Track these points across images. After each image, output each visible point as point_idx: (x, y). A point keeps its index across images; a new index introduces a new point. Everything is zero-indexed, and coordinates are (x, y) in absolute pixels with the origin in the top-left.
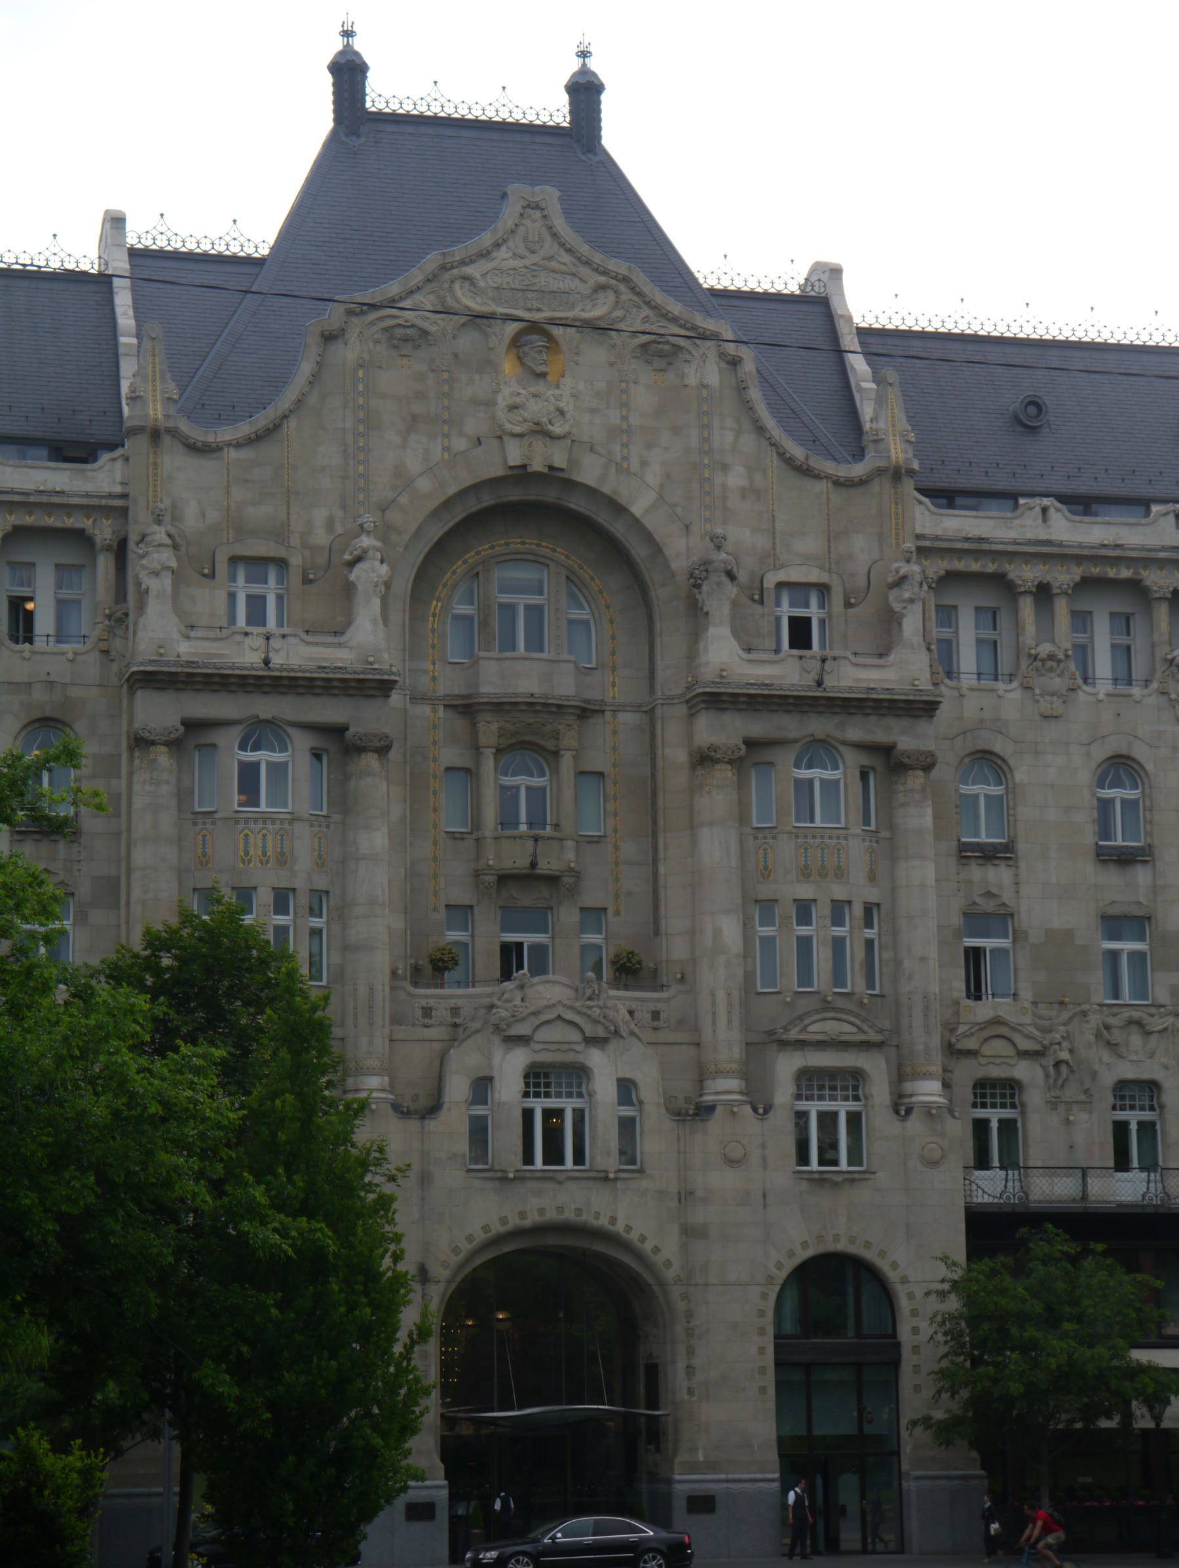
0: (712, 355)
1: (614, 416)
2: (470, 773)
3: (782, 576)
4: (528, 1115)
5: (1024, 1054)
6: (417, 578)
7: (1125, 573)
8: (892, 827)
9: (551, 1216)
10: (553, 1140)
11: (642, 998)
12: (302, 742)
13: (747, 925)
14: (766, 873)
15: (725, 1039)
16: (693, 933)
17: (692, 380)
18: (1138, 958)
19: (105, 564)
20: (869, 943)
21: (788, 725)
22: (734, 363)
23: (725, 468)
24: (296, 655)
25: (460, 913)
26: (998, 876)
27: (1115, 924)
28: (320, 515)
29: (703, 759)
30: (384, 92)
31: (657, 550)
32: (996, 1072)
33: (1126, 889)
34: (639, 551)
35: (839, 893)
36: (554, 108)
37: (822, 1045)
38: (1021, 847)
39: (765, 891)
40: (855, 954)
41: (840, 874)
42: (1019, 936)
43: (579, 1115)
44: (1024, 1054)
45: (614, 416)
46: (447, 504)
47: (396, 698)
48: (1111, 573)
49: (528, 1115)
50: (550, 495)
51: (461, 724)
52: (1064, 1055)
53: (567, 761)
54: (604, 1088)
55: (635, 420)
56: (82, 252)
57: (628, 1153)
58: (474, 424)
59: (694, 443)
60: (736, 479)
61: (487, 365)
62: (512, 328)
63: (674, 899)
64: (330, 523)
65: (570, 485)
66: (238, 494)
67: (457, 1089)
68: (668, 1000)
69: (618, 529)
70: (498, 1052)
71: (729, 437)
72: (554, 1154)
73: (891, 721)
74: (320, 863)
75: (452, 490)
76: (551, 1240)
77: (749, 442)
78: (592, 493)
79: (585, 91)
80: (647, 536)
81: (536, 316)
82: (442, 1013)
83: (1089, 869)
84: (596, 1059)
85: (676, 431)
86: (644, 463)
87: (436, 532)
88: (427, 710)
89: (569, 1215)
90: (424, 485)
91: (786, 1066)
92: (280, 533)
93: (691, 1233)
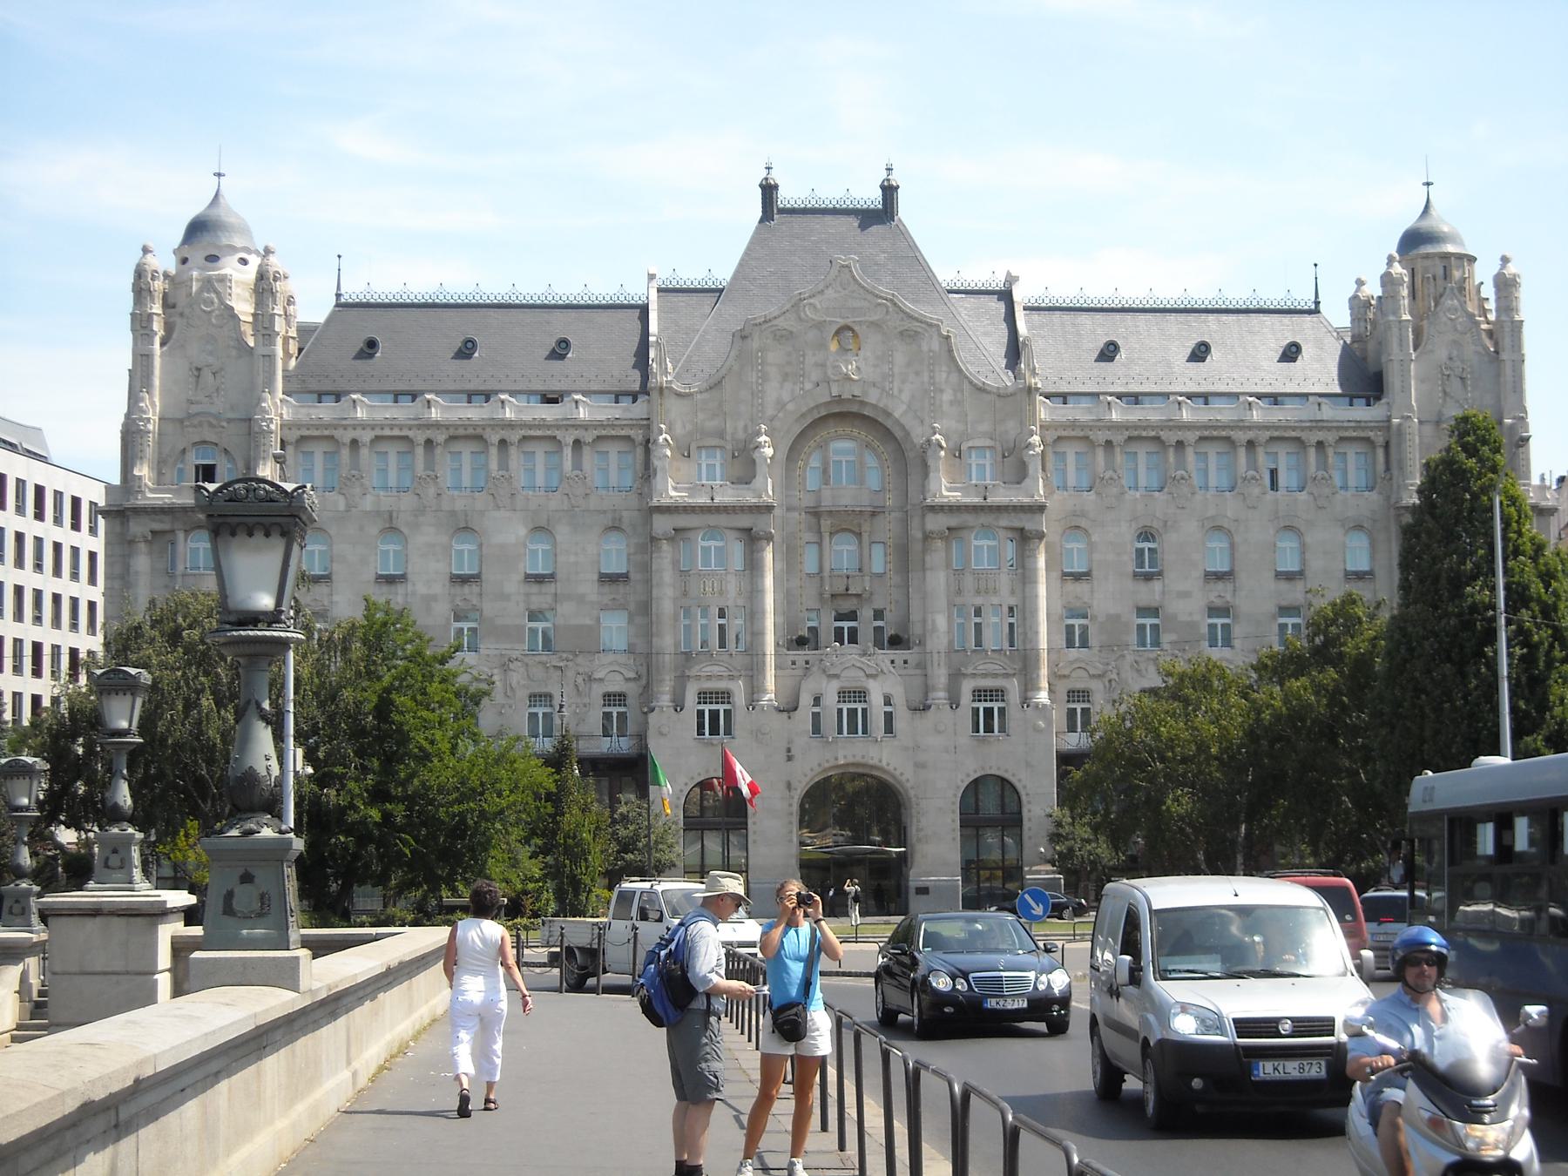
0: (935, 337)
1: (886, 368)
2: (820, 544)
3: (970, 444)
4: (840, 711)
5: (1093, 676)
6: (791, 449)
7: (1153, 434)
8: (1023, 567)
9: (851, 760)
10: (855, 723)
11: (899, 655)
12: (732, 535)
13: (950, 617)
14: (959, 592)
15: (940, 676)
16: (924, 621)
17: (925, 348)
18: (1155, 628)
19: (640, 451)
20: (1011, 625)
21: (969, 519)
22: (948, 337)
23: (942, 391)
24: (726, 496)
26: (1081, 588)
27: (1143, 611)
28: (741, 424)
29: (927, 537)
30: (788, 195)
31: (907, 434)
32: (1080, 686)
33: (1150, 593)
34: (898, 434)
35: (995, 601)
36: (873, 197)
37: (985, 676)
38: (1094, 573)
39: (958, 600)
41: (995, 591)
42: (1094, 618)
43: (864, 711)
44: (1093, 676)
45: (886, 368)
46: (803, 415)
47: (777, 512)
48: (1144, 434)
49: (840, 711)
50: (855, 408)
51: (813, 520)
52: (1114, 676)
53: (865, 536)
54: (876, 699)
55: (896, 370)
56: (637, 289)
57: (889, 728)
58: (815, 375)
59: (926, 379)
61: (822, 346)
62: (834, 328)
63: (915, 603)
64: (746, 427)
65: (862, 403)
66: (701, 416)
67: (806, 700)
68: (911, 655)
69: (889, 424)
70: (824, 681)
71: (944, 375)
72: (853, 729)
73: (1022, 515)
75: (804, 409)
76: (852, 770)
77: (954, 378)
78: (875, 407)
79: (889, 191)
80: (903, 427)
81: (848, 321)
82: (800, 662)
83: (1130, 584)
85: (917, 374)
86: (900, 391)
87: (798, 429)
88: (796, 515)
89: (858, 759)
90: (790, 407)
91: (967, 687)
92: (721, 434)
93: (920, 766)
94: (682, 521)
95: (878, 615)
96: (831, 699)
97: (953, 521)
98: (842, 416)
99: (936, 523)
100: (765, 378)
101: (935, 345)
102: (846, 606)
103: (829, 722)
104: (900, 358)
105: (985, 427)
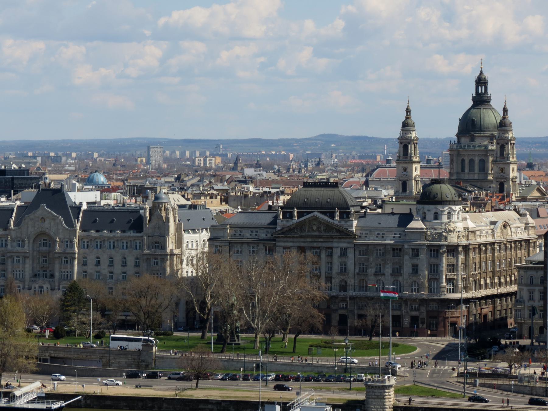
2: (39, 258)
15: (57, 284)
25: (39, 271)
27: (97, 272)
35: (67, 270)
40: (69, 276)
54: (45, 288)
60: (61, 231)
67: (33, 288)
74: (22, 267)
84: (44, 285)
87: (34, 237)
94: (13, 254)
95: (50, 271)
96: (37, 288)
97: (59, 255)
98: (41, 234)
99: (56, 255)
100: (28, 227)
101: (59, 221)
102: (45, 269)
103: (37, 292)
104: (52, 223)
105: (68, 237)
